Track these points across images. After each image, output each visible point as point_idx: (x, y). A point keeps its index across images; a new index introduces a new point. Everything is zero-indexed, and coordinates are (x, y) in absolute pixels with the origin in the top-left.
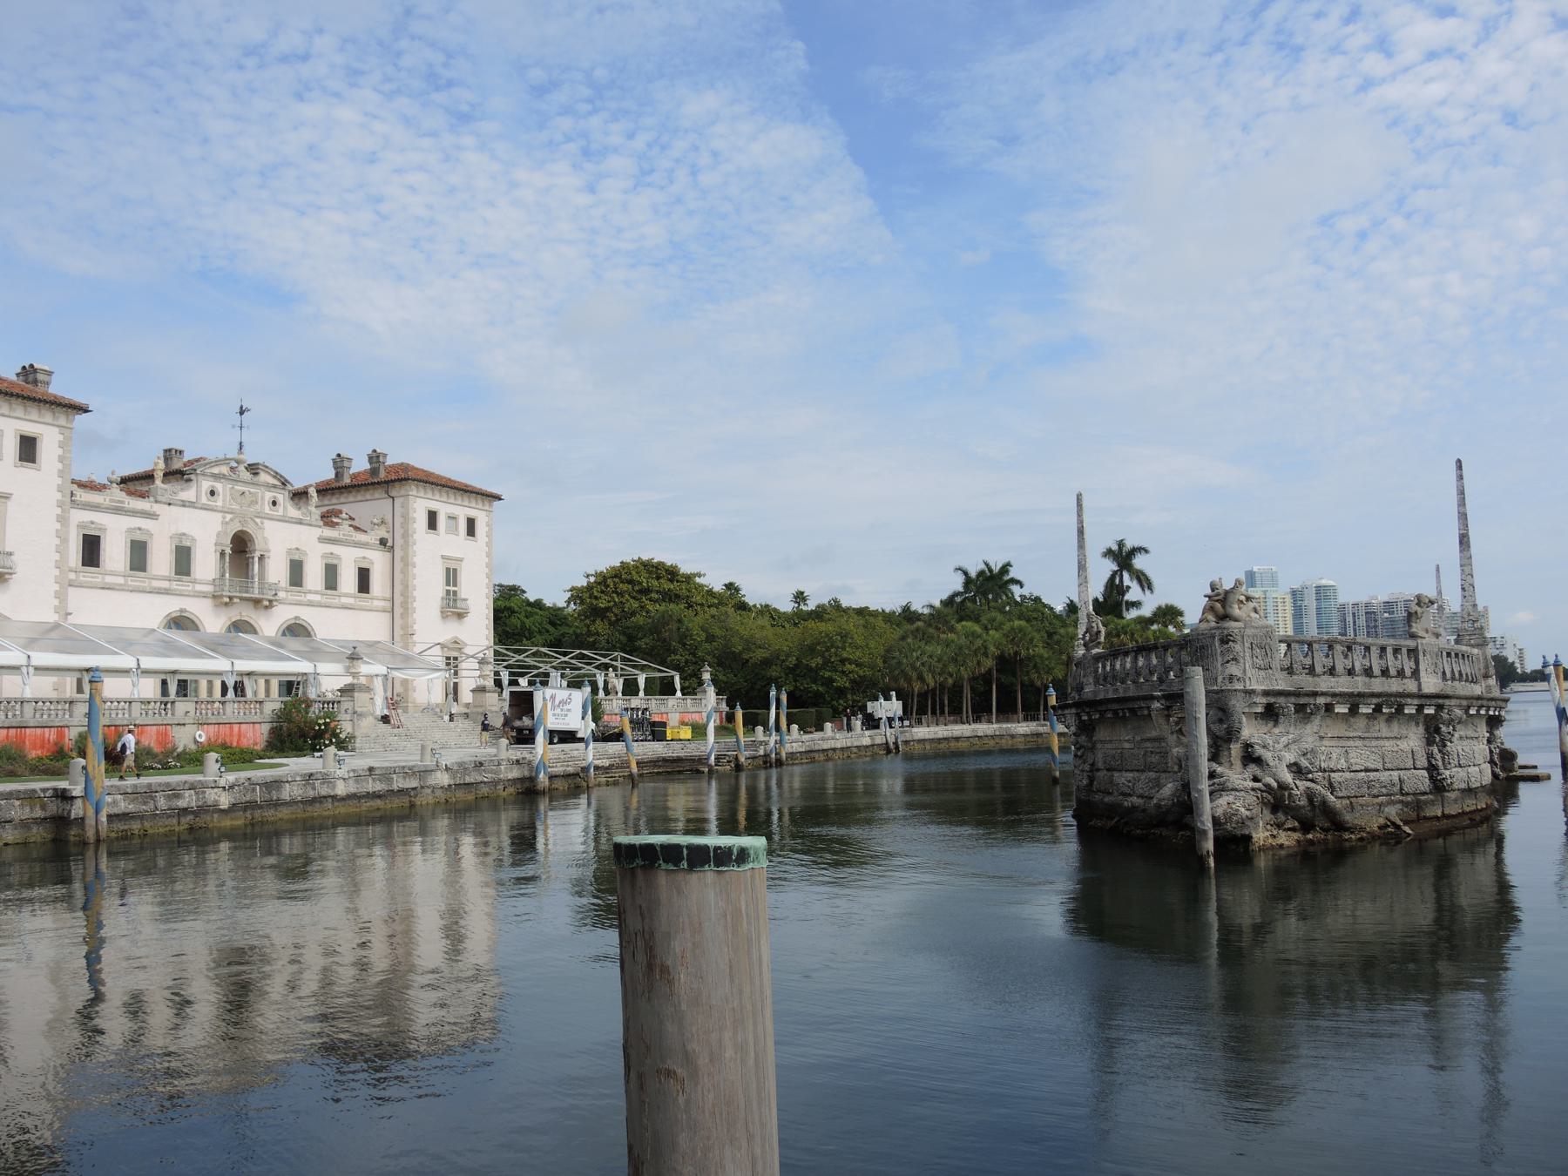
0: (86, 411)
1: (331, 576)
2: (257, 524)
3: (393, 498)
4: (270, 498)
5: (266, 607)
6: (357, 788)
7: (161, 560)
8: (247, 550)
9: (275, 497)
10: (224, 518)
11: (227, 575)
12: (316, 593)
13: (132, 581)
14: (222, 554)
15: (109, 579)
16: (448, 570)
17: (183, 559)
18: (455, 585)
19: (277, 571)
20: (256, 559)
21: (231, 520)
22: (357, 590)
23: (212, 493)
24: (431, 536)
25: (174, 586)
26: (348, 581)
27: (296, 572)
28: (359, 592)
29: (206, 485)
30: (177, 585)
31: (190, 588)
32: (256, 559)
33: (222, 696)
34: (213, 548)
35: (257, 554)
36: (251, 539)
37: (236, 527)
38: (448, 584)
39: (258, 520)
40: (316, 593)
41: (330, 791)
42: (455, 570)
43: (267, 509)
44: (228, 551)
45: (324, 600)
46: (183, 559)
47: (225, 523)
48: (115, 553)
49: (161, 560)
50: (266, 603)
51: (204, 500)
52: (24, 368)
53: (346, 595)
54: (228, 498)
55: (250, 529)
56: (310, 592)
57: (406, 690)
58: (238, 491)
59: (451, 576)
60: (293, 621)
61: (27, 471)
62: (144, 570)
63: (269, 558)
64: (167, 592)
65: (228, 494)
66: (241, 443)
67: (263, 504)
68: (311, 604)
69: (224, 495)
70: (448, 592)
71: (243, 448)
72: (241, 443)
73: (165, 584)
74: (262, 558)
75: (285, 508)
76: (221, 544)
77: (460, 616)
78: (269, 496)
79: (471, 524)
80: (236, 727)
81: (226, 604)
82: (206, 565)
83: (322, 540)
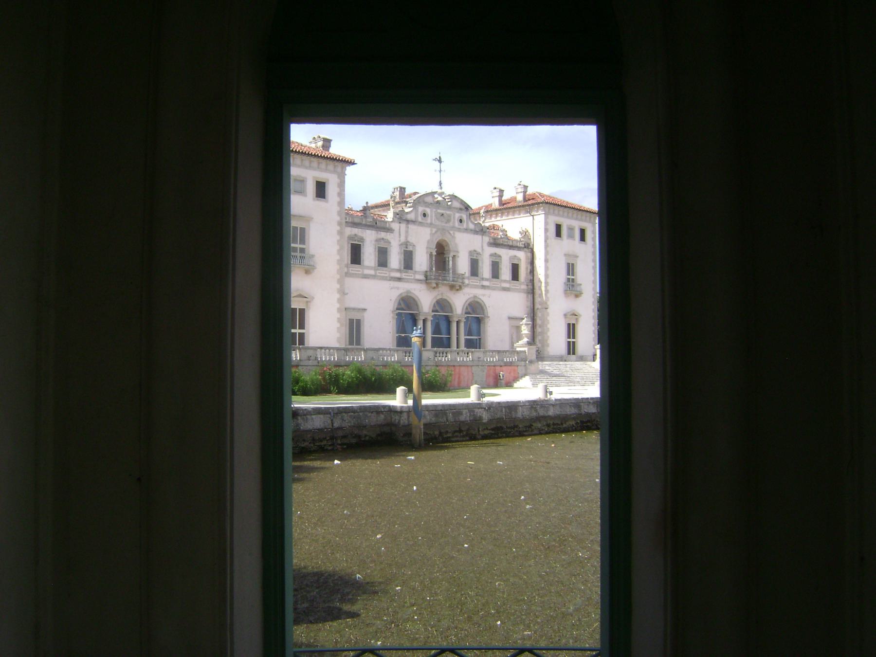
0: (354, 164)
2: (450, 234)
3: (533, 216)
4: (458, 217)
5: (457, 290)
6: (561, 411)
7: (395, 260)
8: (445, 252)
9: (461, 217)
10: (431, 230)
11: (434, 269)
12: (487, 280)
13: (379, 273)
14: (431, 255)
15: (367, 272)
16: (568, 264)
18: (573, 275)
19: (463, 266)
20: (451, 258)
21: (436, 232)
22: (511, 279)
23: (425, 215)
24: (558, 240)
25: (404, 275)
26: (506, 273)
30: (405, 275)
31: (412, 278)
32: (451, 258)
33: (457, 348)
34: (425, 251)
35: (452, 254)
36: (447, 245)
37: (438, 238)
38: (568, 274)
41: (545, 413)
42: (573, 265)
43: (457, 224)
44: (435, 253)
47: (432, 235)
48: (369, 255)
49: (395, 260)
50: (458, 288)
51: (420, 219)
52: (314, 138)
53: (505, 281)
54: (434, 218)
55: (447, 238)
56: (483, 279)
57: (543, 346)
58: (439, 213)
59: (571, 269)
60: (472, 300)
61: (320, 203)
62: (411, 269)
63: (458, 257)
64: (399, 279)
65: (434, 215)
66: (440, 181)
67: (454, 222)
68: (483, 287)
69: (431, 216)
70: (568, 279)
71: (439, 182)
72: (440, 181)
73: (398, 275)
75: (467, 223)
76: (430, 248)
77: (578, 295)
78: (457, 215)
79: (583, 232)
80: (457, 368)
81: (434, 288)
82: (422, 261)
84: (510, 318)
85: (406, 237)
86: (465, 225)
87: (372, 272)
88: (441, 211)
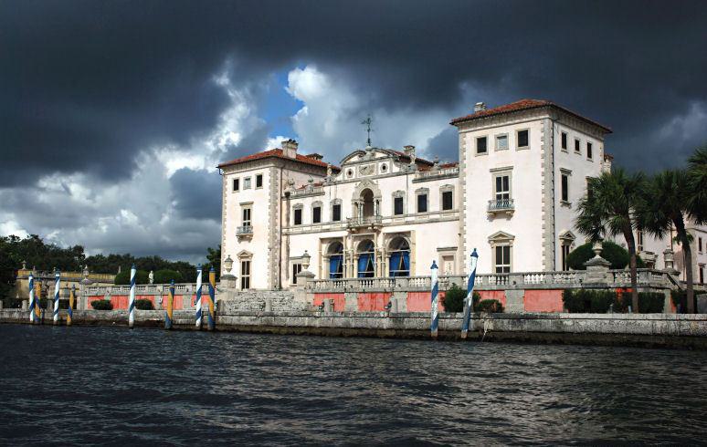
1: (422, 202)
7: (326, 215)
12: (411, 215)
15: (305, 229)
17: (337, 211)
27: (399, 205)
28: (444, 209)
29: (347, 170)
37: (363, 188)
39: (375, 181)
40: (411, 215)
45: (418, 219)
46: (337, 211)
49: (326, 215)
55: (370, 187)
73: (328, 227)
74: (378, 202)
78: (380, 164)
82: (347, 211)
83: (415, 181)
84: (439, 250)
85: (335, 195)
86: (388, 171)
87: (309, 229)
88: (364, 166)
